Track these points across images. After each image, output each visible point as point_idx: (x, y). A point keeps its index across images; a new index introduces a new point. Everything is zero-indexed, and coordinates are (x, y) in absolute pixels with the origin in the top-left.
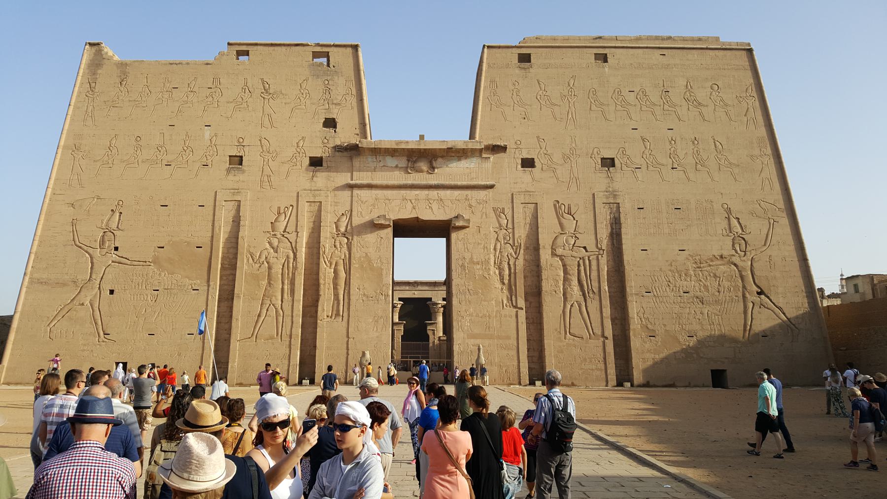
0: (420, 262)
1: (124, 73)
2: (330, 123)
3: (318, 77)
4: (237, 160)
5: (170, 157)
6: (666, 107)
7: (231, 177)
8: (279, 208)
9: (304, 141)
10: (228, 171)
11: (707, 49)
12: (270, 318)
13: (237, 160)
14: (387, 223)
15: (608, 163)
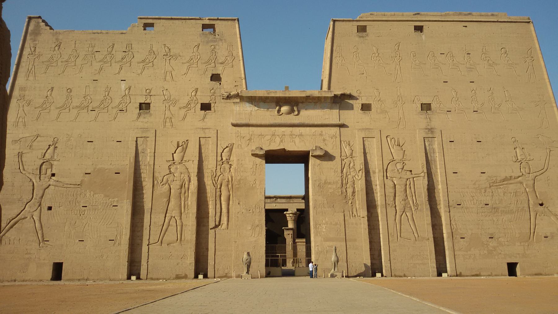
0: (285, 181)
1: (57, 39)
2: (216, 78)
3: (208, 42)
4: (144, 107)
5: (95, 104)
6: (468, 65)
7: (141, 119)
8: (178, 143)
9: (196, 92)
10: (140, 115)
11: (498, 22)
12: (172, 227)
13: (144, 107)
14: (262, 152)
15: (426, 107)
